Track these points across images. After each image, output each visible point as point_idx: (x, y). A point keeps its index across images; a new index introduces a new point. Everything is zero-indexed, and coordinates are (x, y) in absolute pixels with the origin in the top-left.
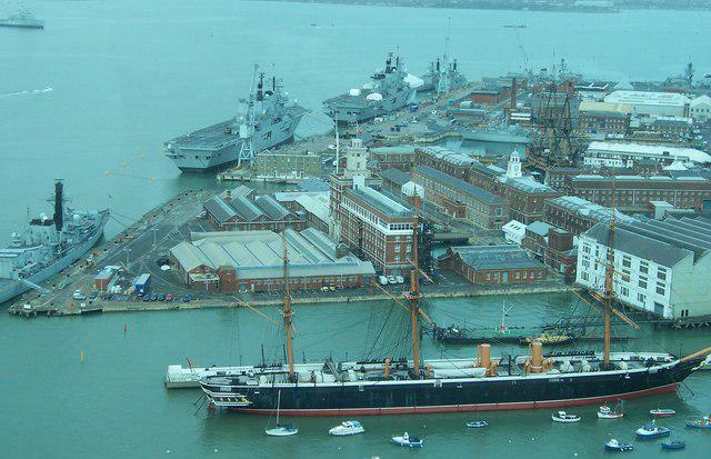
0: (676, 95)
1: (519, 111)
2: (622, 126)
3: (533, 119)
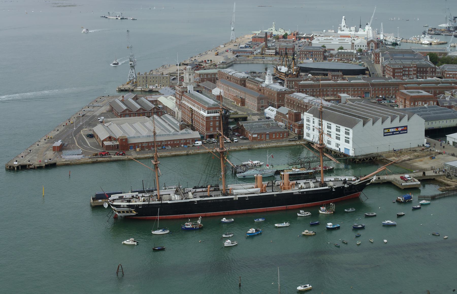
0: (347, 39)
1: (269, 49)
3: (277, 53)
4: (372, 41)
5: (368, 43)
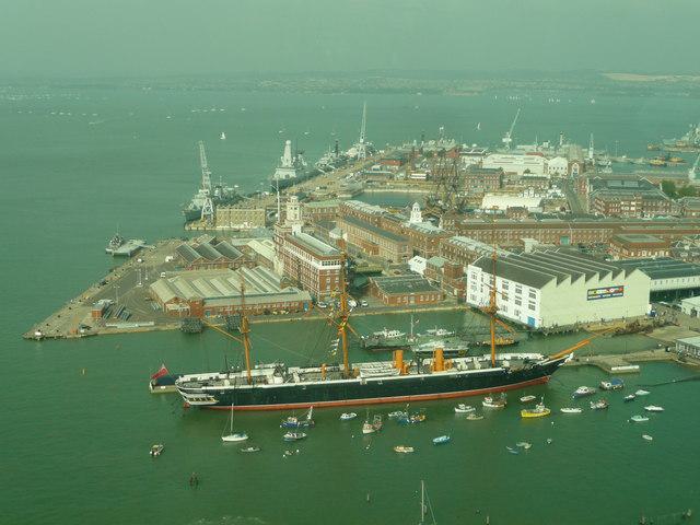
2: (502, 181)
3: (428, 178)
4: (575, 161)
5: (570, 165)
